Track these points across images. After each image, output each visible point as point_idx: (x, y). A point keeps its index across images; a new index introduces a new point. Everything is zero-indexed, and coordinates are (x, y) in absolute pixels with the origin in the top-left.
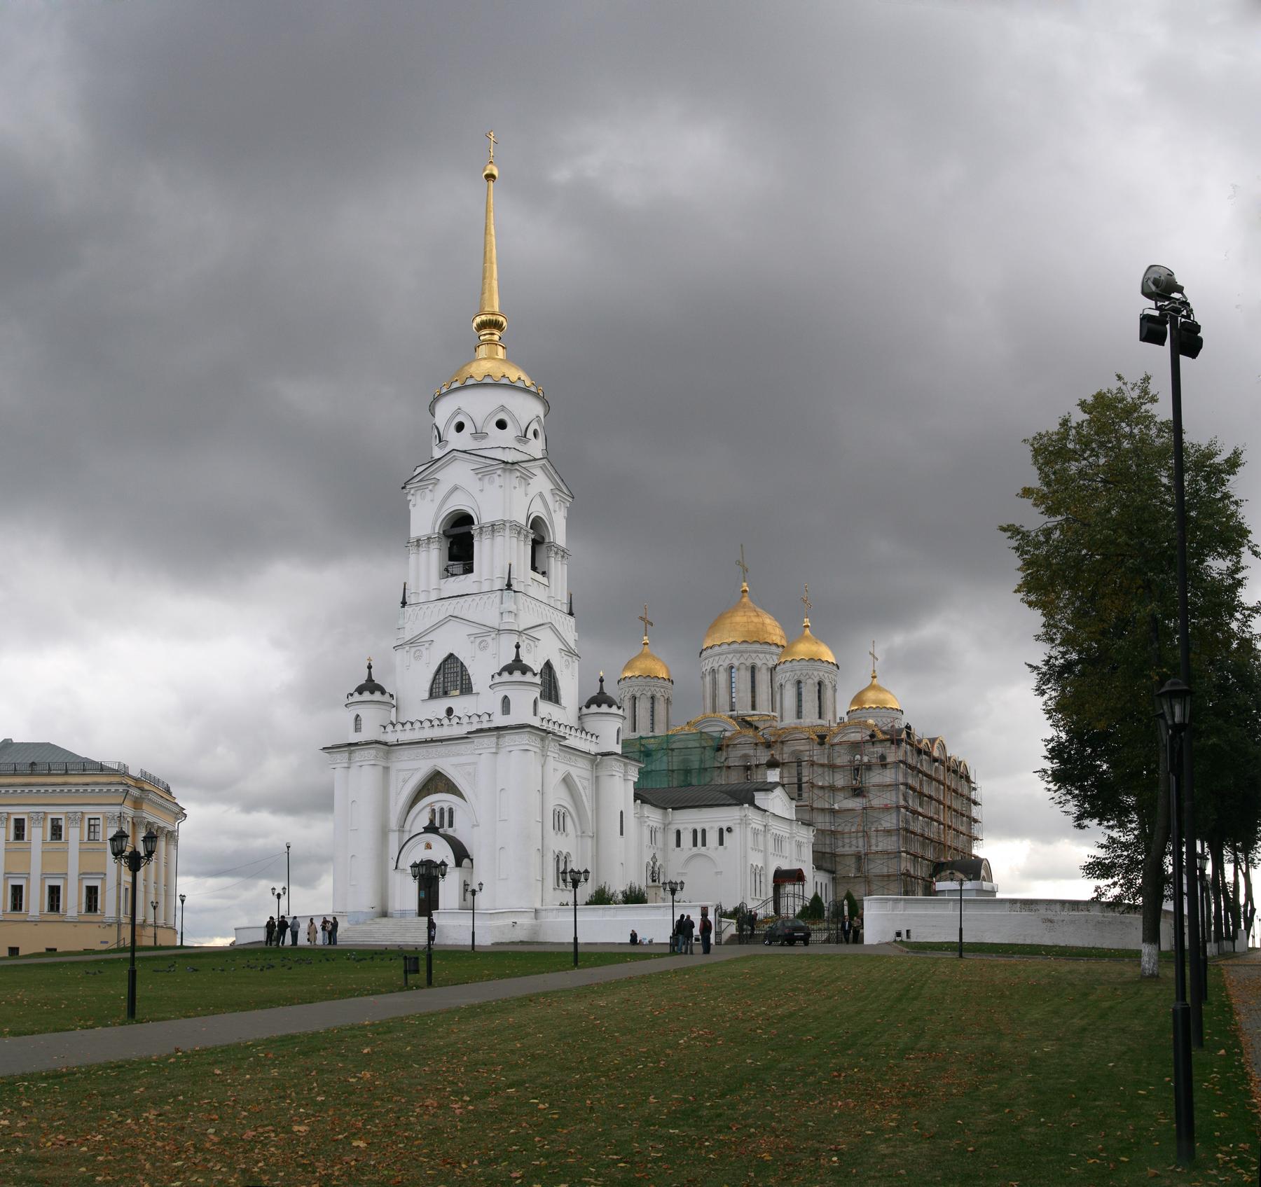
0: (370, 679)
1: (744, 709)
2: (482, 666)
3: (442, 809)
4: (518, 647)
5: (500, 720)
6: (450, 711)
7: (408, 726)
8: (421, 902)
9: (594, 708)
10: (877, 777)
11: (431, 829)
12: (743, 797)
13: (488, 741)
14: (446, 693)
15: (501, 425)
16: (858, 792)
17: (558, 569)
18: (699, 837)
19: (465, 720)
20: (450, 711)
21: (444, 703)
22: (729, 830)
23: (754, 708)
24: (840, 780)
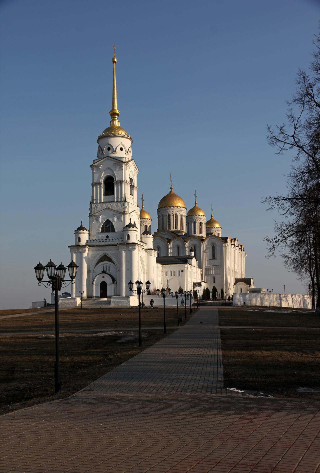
0: (81, 225)
1: (172, 229)
4: (130, 219)
6: (107, 237)
7: (95, 241)
8: (101, 293)
9: (145, 235)
11: (104, 272)
12: (185, 260)
14: (106, 231)
15: (121, 149)
17: (135, 192)
19: (114, 240)
20: (107, 237)
22: (182, 271)
23: (176, 228)
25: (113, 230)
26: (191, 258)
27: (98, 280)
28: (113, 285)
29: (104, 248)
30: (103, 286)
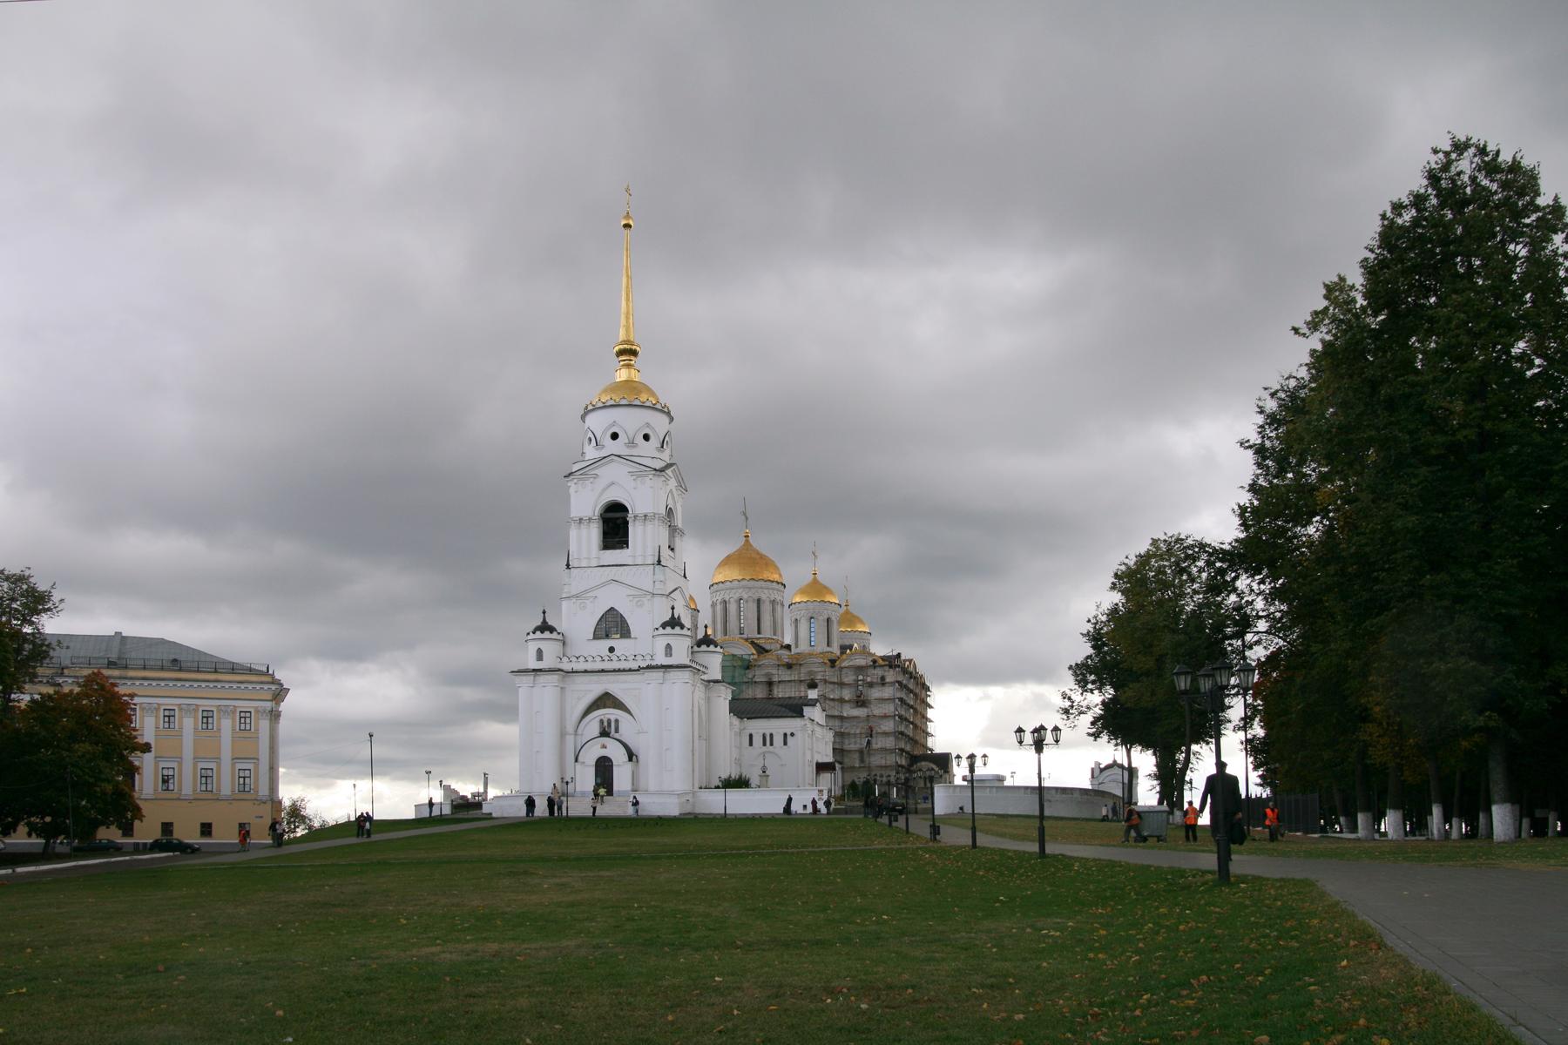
2: (644, 619)
3: (609, 722)
5: (661, 659)
6: (612, 650)
9: (704, 648)
10: (875, 693)
11: (604, 733)
12: (795, 709)
13: (658, 675)
14: (607, 636)
15: (646, 437)
16: (861, 702)
18: (768, 740)
20: (612, 650)
21: (608, 643)
24: (847, 694)
25: (625, 633)
26: (812, 703)
27: (591, 755)
28: (629, 766)
29: (604, 677)
30: (604, 768)
